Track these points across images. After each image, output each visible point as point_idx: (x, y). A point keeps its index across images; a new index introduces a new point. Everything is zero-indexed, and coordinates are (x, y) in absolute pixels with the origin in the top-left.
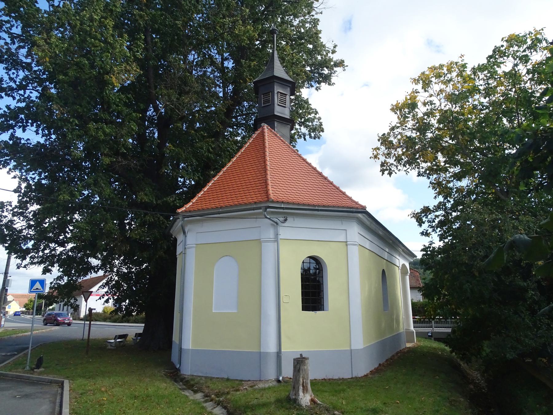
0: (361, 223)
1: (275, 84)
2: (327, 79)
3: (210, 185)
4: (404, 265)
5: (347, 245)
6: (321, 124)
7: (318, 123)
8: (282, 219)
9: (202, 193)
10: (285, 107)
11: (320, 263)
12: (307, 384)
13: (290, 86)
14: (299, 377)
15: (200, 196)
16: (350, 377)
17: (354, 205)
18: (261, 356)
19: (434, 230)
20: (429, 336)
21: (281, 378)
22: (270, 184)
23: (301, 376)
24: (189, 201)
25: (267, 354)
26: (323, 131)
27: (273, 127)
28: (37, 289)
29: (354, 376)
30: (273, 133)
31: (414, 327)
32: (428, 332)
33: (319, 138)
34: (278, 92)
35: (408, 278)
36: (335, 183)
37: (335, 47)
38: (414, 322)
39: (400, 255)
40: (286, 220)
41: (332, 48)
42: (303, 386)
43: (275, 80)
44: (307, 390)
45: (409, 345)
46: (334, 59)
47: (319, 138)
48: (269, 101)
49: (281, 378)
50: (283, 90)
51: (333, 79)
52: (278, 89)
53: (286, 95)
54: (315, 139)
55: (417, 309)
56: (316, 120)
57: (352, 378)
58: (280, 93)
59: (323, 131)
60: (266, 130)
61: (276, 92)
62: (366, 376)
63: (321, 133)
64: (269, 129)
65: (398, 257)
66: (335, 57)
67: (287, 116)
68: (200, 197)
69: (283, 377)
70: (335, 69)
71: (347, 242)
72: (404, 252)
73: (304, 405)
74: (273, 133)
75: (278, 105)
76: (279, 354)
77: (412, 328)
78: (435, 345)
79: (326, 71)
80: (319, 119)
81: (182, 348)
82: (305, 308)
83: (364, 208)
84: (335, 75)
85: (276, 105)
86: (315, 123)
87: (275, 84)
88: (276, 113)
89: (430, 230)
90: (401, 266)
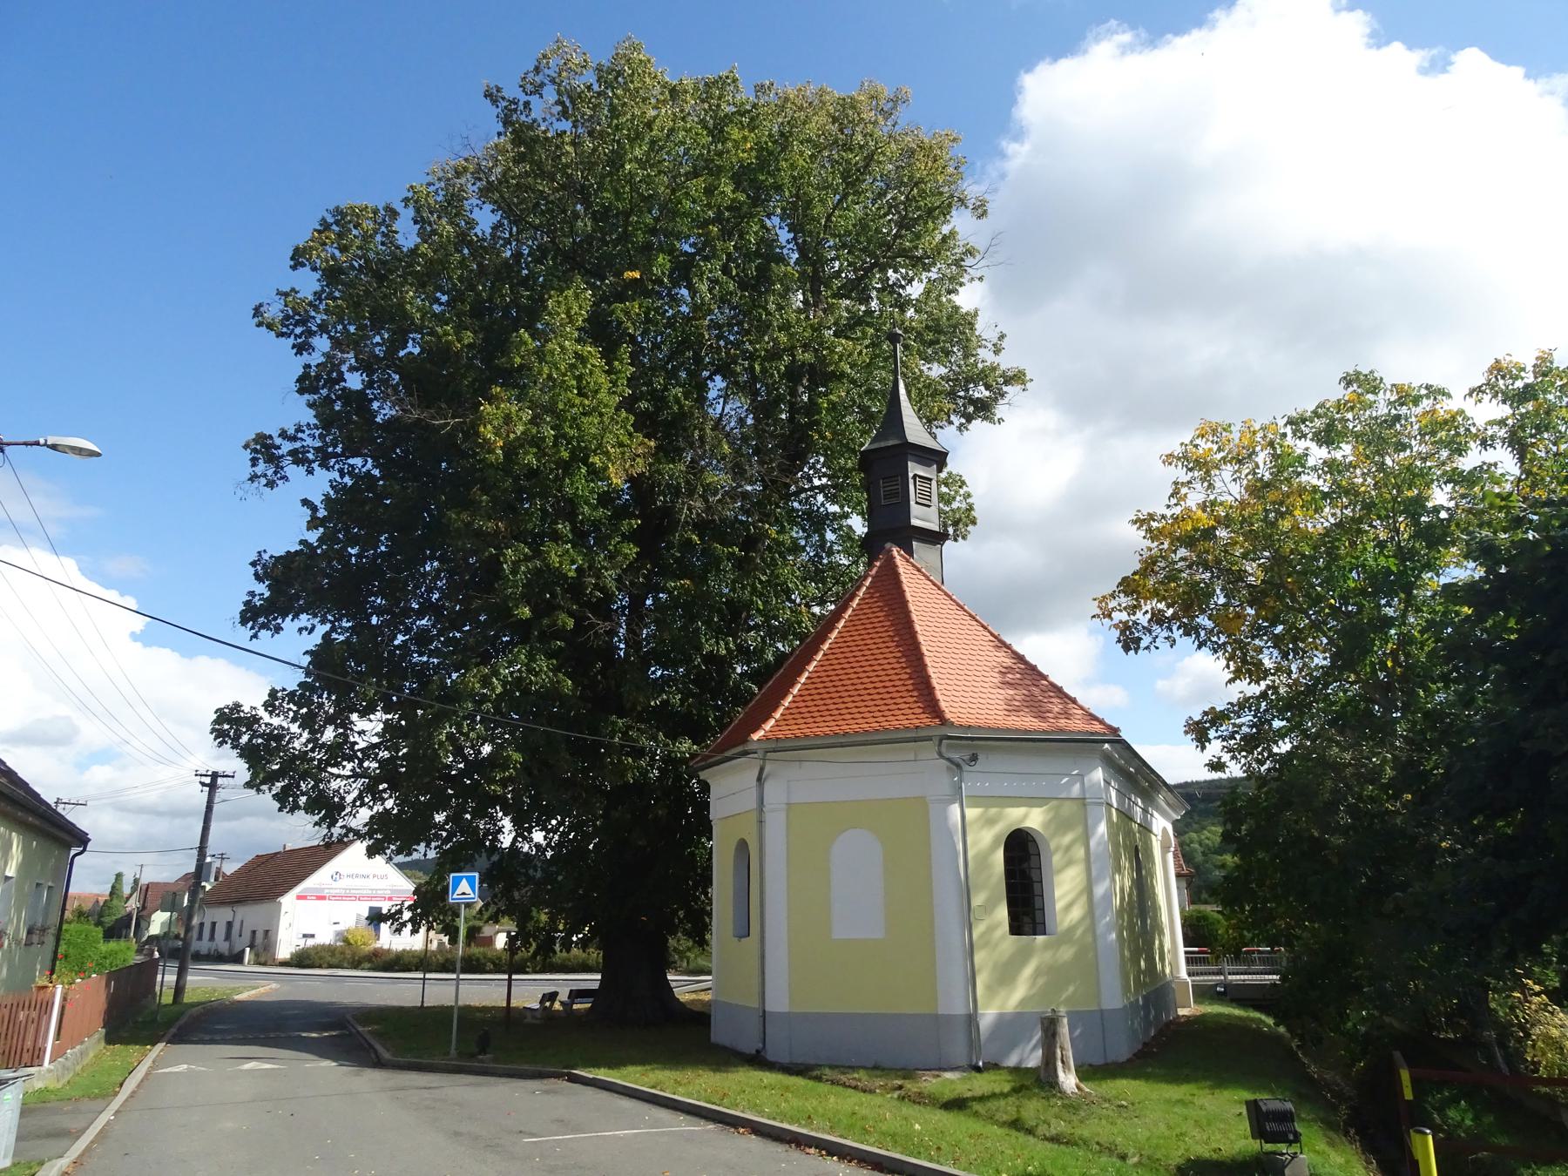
0: (1108, 761)
1: (909, 456)
2: (983, 409)
3: (803, 680)
4: (1164, 830)
5: (1085, 805)
6: (970, 508)
7: (964, 506)
8: (966, 755)
9: (790, 698)
10: (929, 506)
11: (1035, 841)
12: (1068, 1058)
13: (937, 459)
14: (1055, 1047)
15: (787, 704)
16: (1101, 1062)
17: (1098, 727)
18: (939, 1022)
19: (1233, 758)
20: (1220, 993)
21: (981, 1064)
22: (937, 687)
23: (1058, 1045)
24: (769, 717)
25: (949, 1018)
26: (974, 522)
27: (910, 552)
28: (464, 894)
29: (1109, 1061)
30: (913, 565)
31: (1189, 975)
32: (1216, 985)
33: (964, 538)
34: (915, 476)
35: (1170, 856)
36: (1028, 658)
37: (1002, 337)
38: (1189, 961)
39: (1158, 809)
40: (974, 758)
41: (995, 340)
42: (1063, 1062)
43: (910, 451)
44: (1069, 1070)
45: (1182, 1012)
46: (1003, 367)
47: (964, 538)
48: (895, 494)
49: (981, 1064)
50: (923, 470)
51: (1000, 410)
52: (914, 469)
53: (930, 480)
54: (956, 540)
55: (1196, 932)
56: (958, 498)
57: (1107, 1064)
58: (921, 477)
59: (974, 522)
60: (899, 561)
61: (911, 475)
62: (1129, 1061)
63: (970, 528)
64: (901, 556)
65: (1155, 813)
66: (1006, 362)
67: (934, 526)
68: (788, 708)
69: (984, 1063)
70: (1005, 389)
71: (1085, 799)
72: (1168, 804)
73: (1069, 1092)
74: (913, 565)
75: (917, 503)
76: (972, 1019)
77: (1183, 974)
78: (1237, 1012)
79: (980, 392)
80: (968, 495)
81: (767, 1009)
82: (1016, 928)
83: (1115, 731)
84: (1006, 400)
85: (912, 503)
86: (955, 505)
87: (909, 456)
88: (915, 522)
89: (1226, 757)
90: (1160, 834)
